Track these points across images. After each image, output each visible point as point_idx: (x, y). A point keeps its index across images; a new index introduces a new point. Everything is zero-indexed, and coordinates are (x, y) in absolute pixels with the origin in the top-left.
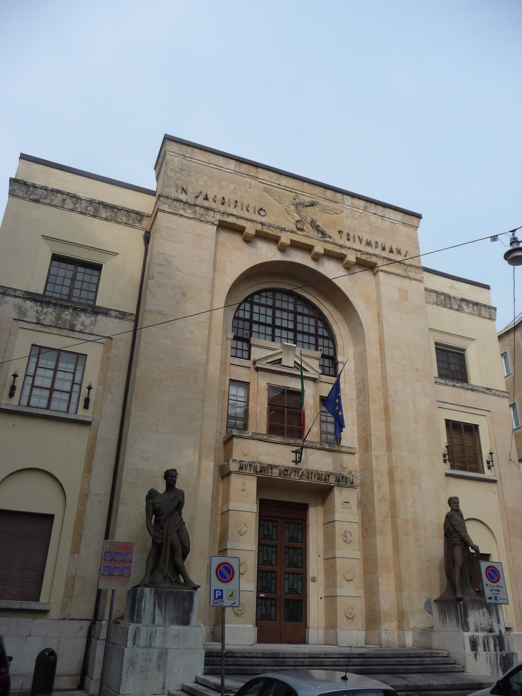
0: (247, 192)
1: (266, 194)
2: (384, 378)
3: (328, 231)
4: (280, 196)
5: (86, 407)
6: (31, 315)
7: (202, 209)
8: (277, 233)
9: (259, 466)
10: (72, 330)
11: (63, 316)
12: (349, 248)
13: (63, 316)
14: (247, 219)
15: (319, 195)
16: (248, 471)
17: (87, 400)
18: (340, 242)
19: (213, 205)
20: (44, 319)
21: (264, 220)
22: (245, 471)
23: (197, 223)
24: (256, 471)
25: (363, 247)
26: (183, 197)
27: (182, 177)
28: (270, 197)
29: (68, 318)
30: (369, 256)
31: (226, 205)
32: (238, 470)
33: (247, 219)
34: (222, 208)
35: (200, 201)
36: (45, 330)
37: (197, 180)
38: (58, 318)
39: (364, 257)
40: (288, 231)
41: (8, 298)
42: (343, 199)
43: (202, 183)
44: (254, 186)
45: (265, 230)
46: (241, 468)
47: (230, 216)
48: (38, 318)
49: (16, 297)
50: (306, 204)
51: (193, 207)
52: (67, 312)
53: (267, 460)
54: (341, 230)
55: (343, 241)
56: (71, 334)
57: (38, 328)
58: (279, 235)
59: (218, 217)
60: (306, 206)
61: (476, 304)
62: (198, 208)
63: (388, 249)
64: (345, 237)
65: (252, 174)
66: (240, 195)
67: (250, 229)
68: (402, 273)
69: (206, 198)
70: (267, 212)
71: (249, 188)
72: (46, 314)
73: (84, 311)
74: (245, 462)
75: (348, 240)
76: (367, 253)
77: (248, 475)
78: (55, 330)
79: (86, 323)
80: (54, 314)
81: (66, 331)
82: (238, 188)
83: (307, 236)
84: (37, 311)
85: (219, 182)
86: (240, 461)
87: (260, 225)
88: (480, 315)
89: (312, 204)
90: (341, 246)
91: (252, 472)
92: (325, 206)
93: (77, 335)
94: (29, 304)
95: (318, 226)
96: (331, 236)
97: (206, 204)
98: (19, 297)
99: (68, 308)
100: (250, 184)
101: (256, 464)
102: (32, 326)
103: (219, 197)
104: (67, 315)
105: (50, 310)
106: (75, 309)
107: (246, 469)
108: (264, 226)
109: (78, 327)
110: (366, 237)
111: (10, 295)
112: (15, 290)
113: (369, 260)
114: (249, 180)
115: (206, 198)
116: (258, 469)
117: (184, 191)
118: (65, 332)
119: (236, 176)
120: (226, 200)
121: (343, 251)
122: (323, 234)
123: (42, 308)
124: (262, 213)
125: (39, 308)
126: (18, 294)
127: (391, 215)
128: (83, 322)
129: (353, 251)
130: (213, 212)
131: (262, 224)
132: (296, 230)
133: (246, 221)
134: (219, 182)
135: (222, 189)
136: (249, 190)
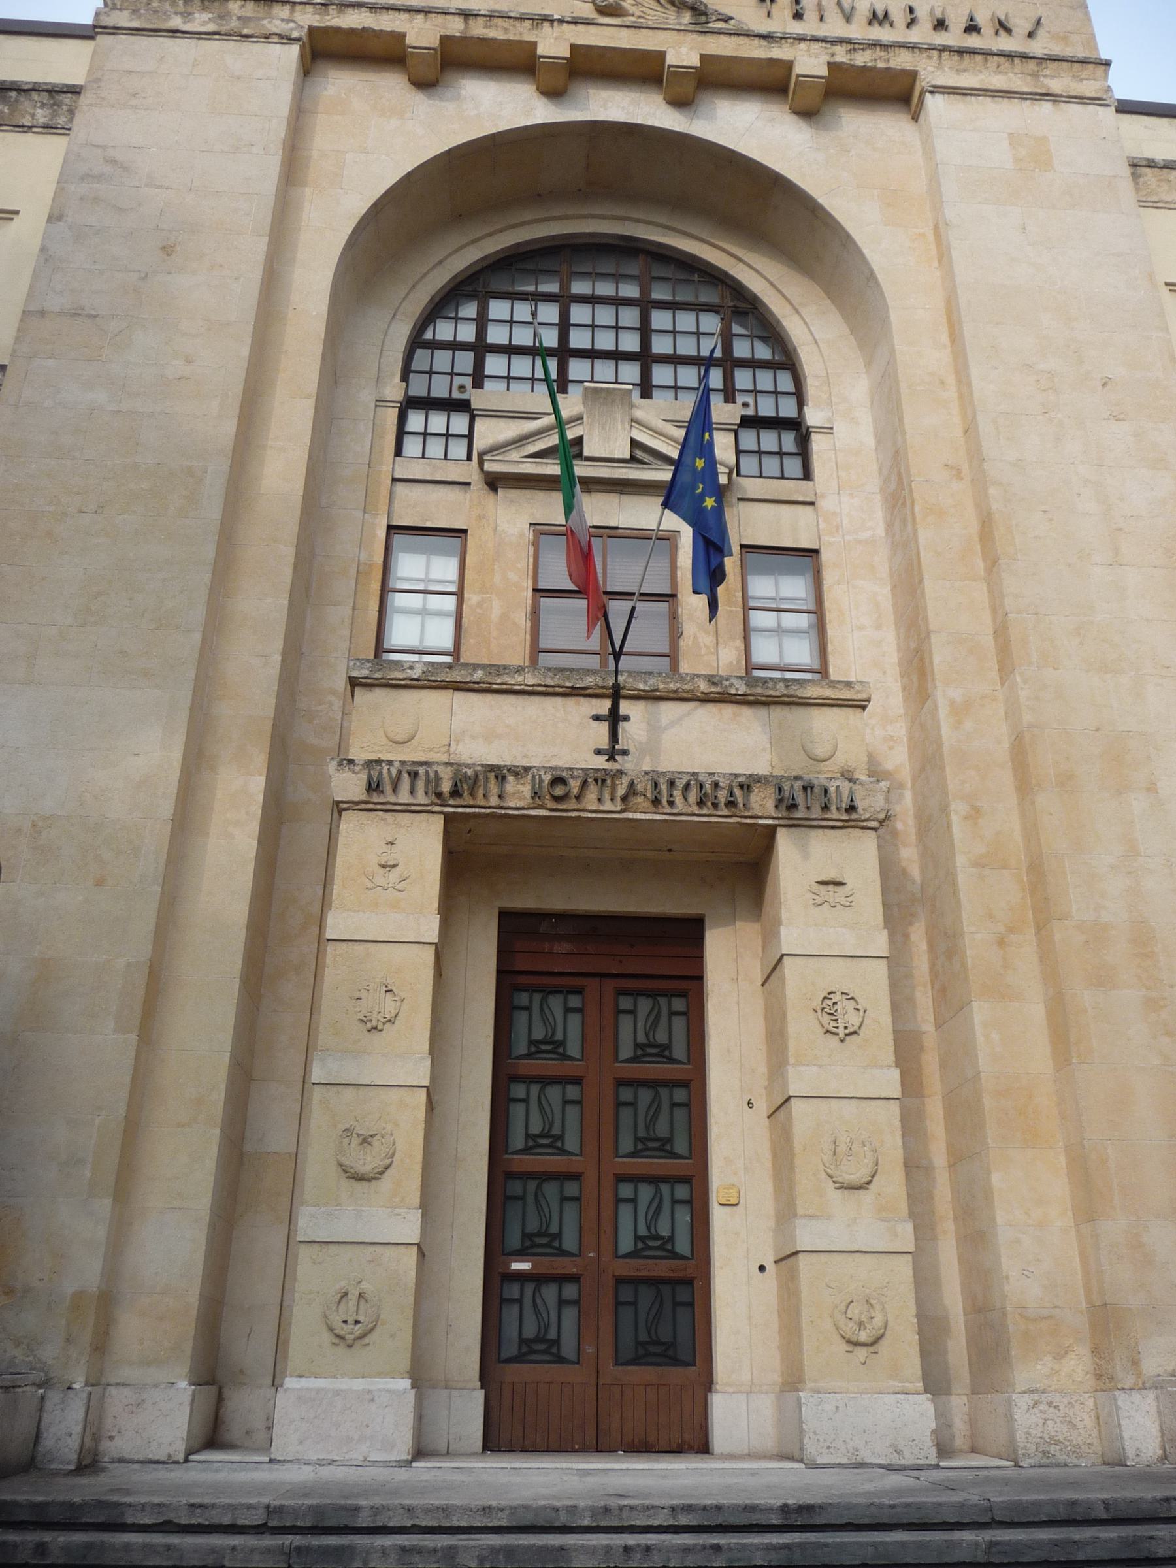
2: (970, 429)
9: (446, 774)
16: (404, 797)
22: (392, 799)
24: (439, 795)
32: (364, 797)
46: (373, 787)
53: (477, 752)
74: (390, 763)
77: (407, 809)
86: (369, 764)
91: (421, 798)
101: (435, 767)
107: (395, 790)
116: (446, 787)
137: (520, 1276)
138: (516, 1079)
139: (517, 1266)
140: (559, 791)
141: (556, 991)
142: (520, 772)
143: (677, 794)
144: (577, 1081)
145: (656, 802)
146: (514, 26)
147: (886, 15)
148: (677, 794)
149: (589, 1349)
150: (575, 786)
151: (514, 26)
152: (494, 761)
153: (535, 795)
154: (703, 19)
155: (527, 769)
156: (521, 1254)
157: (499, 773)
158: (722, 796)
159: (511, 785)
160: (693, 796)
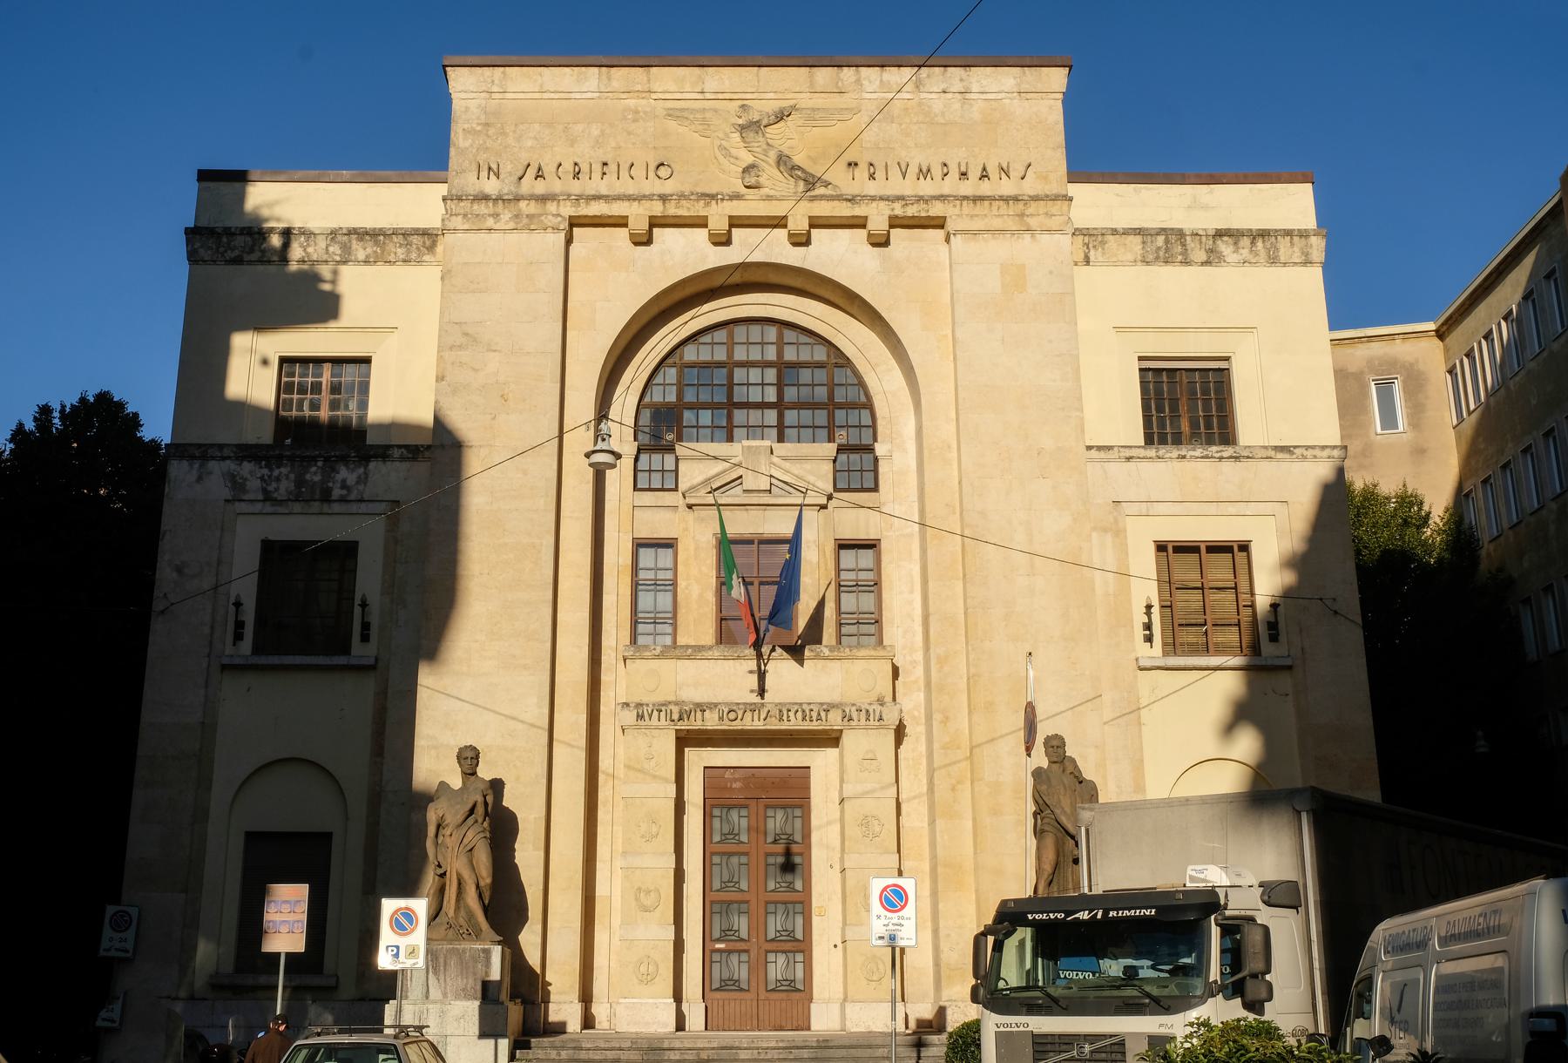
1: (672, 124)
5: (365, 638)
6: (254, 484)
8: (698, 209)
9: (676, 710)
10: (326, 497)
11: (308, 477)
12: (873, 199)
13: (308, 477)
17: (366, 626)
18: (849, 188)
19: (557, 186)
20: (277, 489)
25: (908, 187)
29: (317, 478)
30: (923, 205)
36: (280, 509)
38: (300, 482)
39: (911, 211)
41: (212, 464)
46: (640, 717)
48: (265, 491)
49: (224, 458)
52: (314, 469)
55: (858, 183)
56: (326, 508)
57: (268, 508)
61: (1264, 234)
63: (974, 173)
64: (862, 172)
68: (1011, 224)
72: (278, 479)
73: (344, 459)
75: (872, 177)
76: (920, 199)
78: (297, 507)
79: (349, 483)
80: (292, 476)
81: (317, 504)
83: (769, 198)
84: (262, 478)
88: (1273, 260)
89: (781, 116)
90: (852, 200)
93: (336, 507)
94: (247, 466)
95: (794, 168)
98: (229, 458)
99: (314, 459)
102: (259, 506)
104: (314, 475)
105: (284, 470)
106: (327, 460)
109: (337, 493)
110: (917, 159)
111: (213, 458)
112: (221, 447)
113: (923, 214)
114: (632, 102)
115: (539, 175)
116: (676, 717)
118: (316, 506)
121: (858, 211)
123: (271, 470)
125: (265, 471)
126: (226, 452)
127: (984, 82)
128: (344, 481)
129: (882, 204)
133: (626, 204)
137: (719, 951)
138: (713, 854)
139: (718, 946)
140: (732, 715)
141: (734, 806)
142: (713, 706)
143: (791, 714)
144: (746, 854)
145: (781, 719)
148: (791, 714)
149: (754, 984)
150: (740, 714)
152: (698, 700)
153: (721, 719)
155: (716, 705)
156: (719, 940)
157: (702, 708)
158: (814, 715)
159: (707, 713)
160: (799, 714)
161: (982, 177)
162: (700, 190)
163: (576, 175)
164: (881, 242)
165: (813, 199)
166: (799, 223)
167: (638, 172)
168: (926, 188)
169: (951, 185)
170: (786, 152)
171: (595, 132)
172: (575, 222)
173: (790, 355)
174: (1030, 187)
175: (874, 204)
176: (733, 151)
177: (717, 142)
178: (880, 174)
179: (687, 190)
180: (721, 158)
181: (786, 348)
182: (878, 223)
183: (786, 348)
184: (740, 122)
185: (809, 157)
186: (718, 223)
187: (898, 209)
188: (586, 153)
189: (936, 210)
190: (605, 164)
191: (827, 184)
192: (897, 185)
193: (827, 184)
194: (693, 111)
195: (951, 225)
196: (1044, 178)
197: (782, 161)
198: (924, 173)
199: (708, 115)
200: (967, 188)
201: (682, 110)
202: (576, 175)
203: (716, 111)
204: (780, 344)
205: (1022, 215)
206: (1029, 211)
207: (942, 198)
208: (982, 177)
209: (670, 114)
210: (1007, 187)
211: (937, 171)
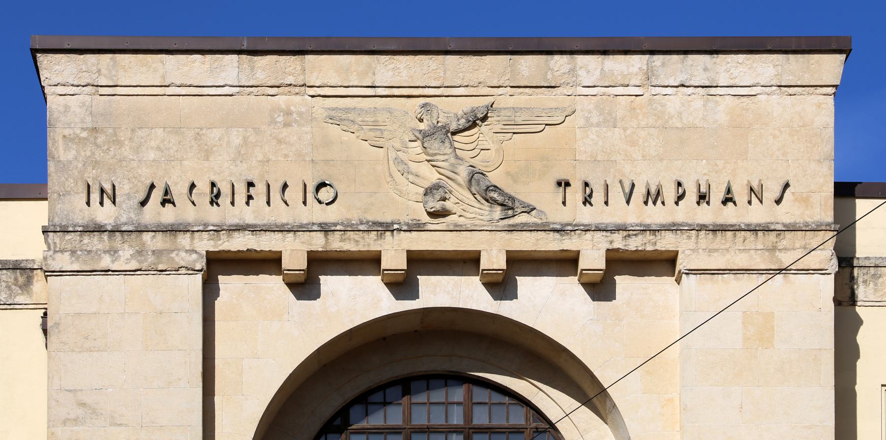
0: (280, 142)
3: (523, 193)
4: (375, 123)
7: (160, 235)
14: (282, 229)
15: (495, 84)
21: (331, 215)
23: (151, 279)
26: (106, 214)
27: (99, 155)
28: (347, 136)
30: (649, 236)
31: (224, 200)
33: (282, 229)
34: (214, 215)
35: (154, 213)
37: (137, 150)
39: (635, 244)
40: (399, 230)
42: (573, 71)
43: (152, 155)
44: (300, 114)
45: (338, 244)
47: (236, 234)
50: (453, 127)
51: (134, 235)
54: (563, 176)
58: (374, 247)
59: (206, 244)
60: (454, 134)
62: (147, 237)
64: (575, 194)
65: (290, 80)
66: (260, 157)
67: (294, 254)
69: (167, 200)
70: (340, 187)
71: (287, 125)
75: (587, 201)
82: (252, 139)
85: (198, 137)
87: (321, 235)
92: (515, 109)
96: (534, 203)
97: (168, 215)
100: (288, 113)
103: (203, 187)
108: (331, 236)
110: (645, 177)
113: (649, 248)
117: (109, 195)
119: (244, 99)
120: (225, 190)
121: (569, 244)
122: (508, 205)
124: (326, 194)
129: (599, 234)
130: (188, 234)
131: (326, 229)
132: (426, 218)
134: (198, 137)
135: (207, 154)
136: (285, 132)
146: (363, 238)
147: (658, 193)
151: (363, 238)
154: (510, 212)
161: (725, 202)
162: (371, 217)
163: (215, 199)
164: (600, 288)
165: (512, 229)
166: (494, 260)
167: (294, 194)
168: (655, 215)
169: (688, 211)
170: (480, 167)
171: (236, 140)
172: (218, 265)
173: (481, 418)
174: (786, 214)
175: (589, 235)
176: (413, 166)
177: (392, 154)
178: (598, 198)
179: (354, 216)
180: (397, 175)
181: (477, 410)
182: (593, 259)
183: (477, 410)
184: (422, 126)
185: (508, 173)
186: (394, 259)
187: (618, 242)
188: (227, 171)
189: (666, 243)
190: (250, 184)
191: (530, 210)
192: (619, 212)
193: (530, 210)
194: (361, 111)
195: (682, 264)
196: (805, 200)
197: (475, 176)
198: (654, 196)
199: (381, 117)
200: (706, 215)
201: (347, 110)
202: (215, 199)
203: (390, 111)
204: (469, 406)
205: (773, 249)
206: (784, 243)
207: (673, 228)
208: (725, 202)
209: (333, 119)
210: (757, 214)
211: (670, 194)
